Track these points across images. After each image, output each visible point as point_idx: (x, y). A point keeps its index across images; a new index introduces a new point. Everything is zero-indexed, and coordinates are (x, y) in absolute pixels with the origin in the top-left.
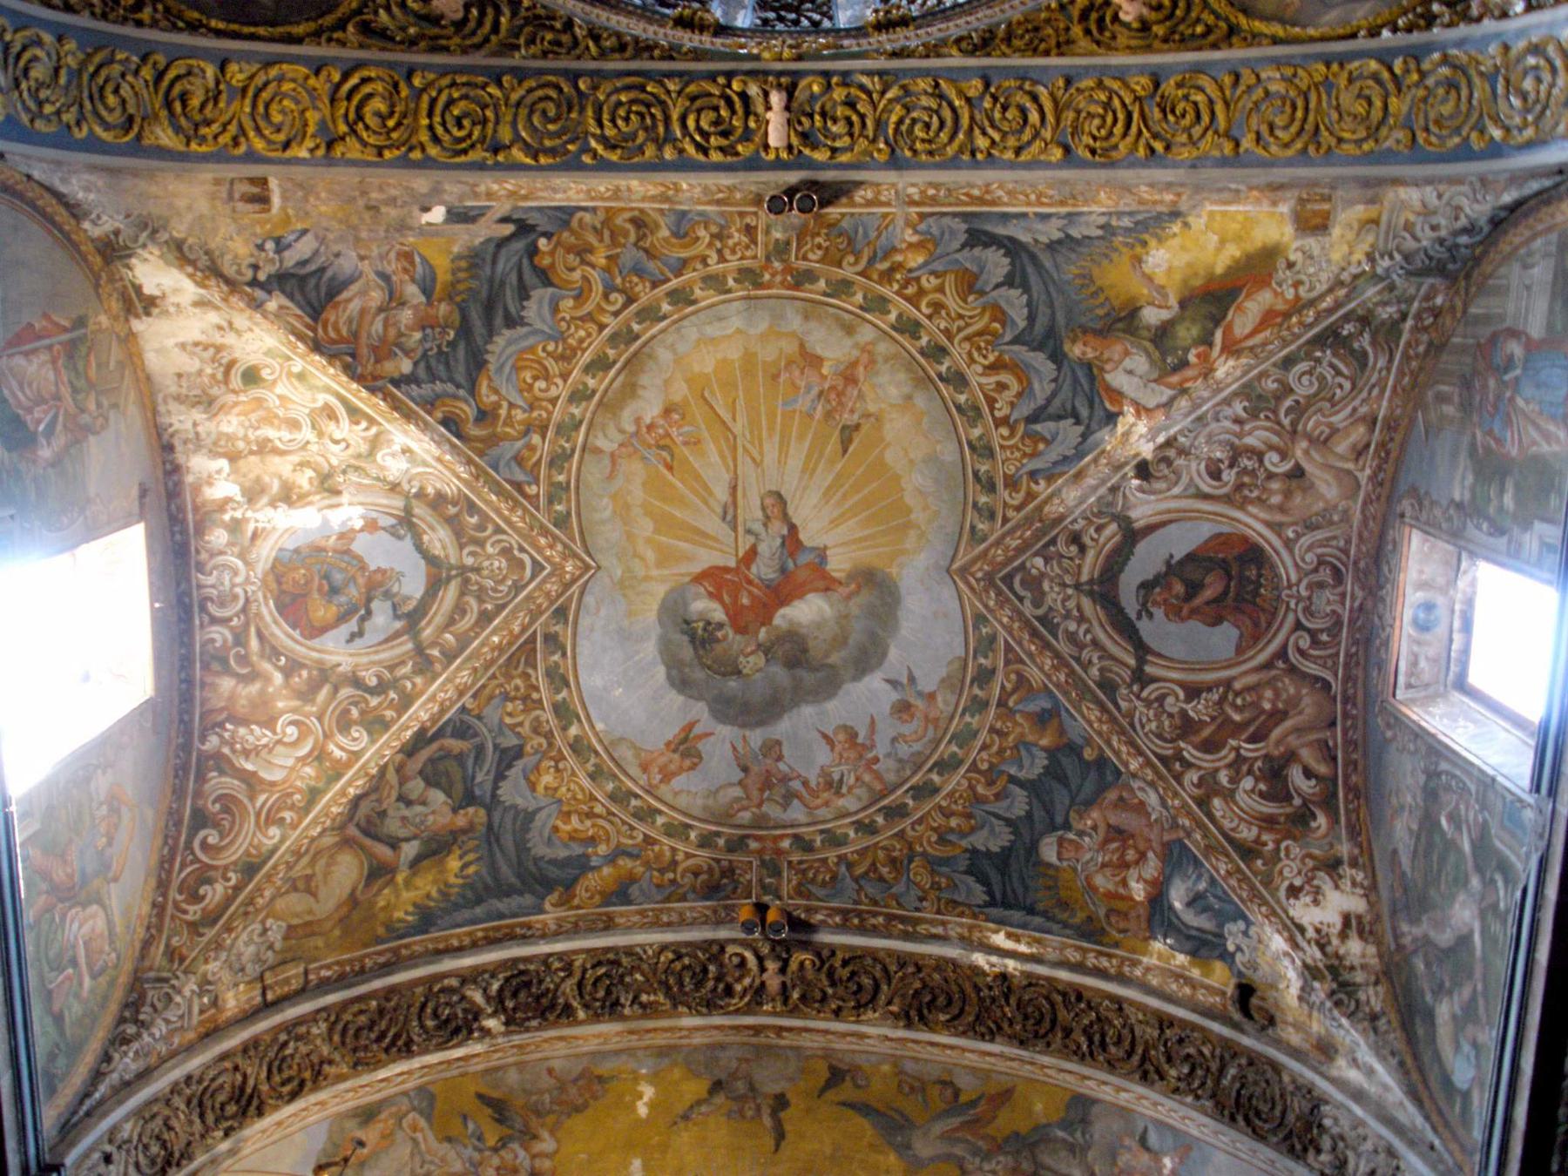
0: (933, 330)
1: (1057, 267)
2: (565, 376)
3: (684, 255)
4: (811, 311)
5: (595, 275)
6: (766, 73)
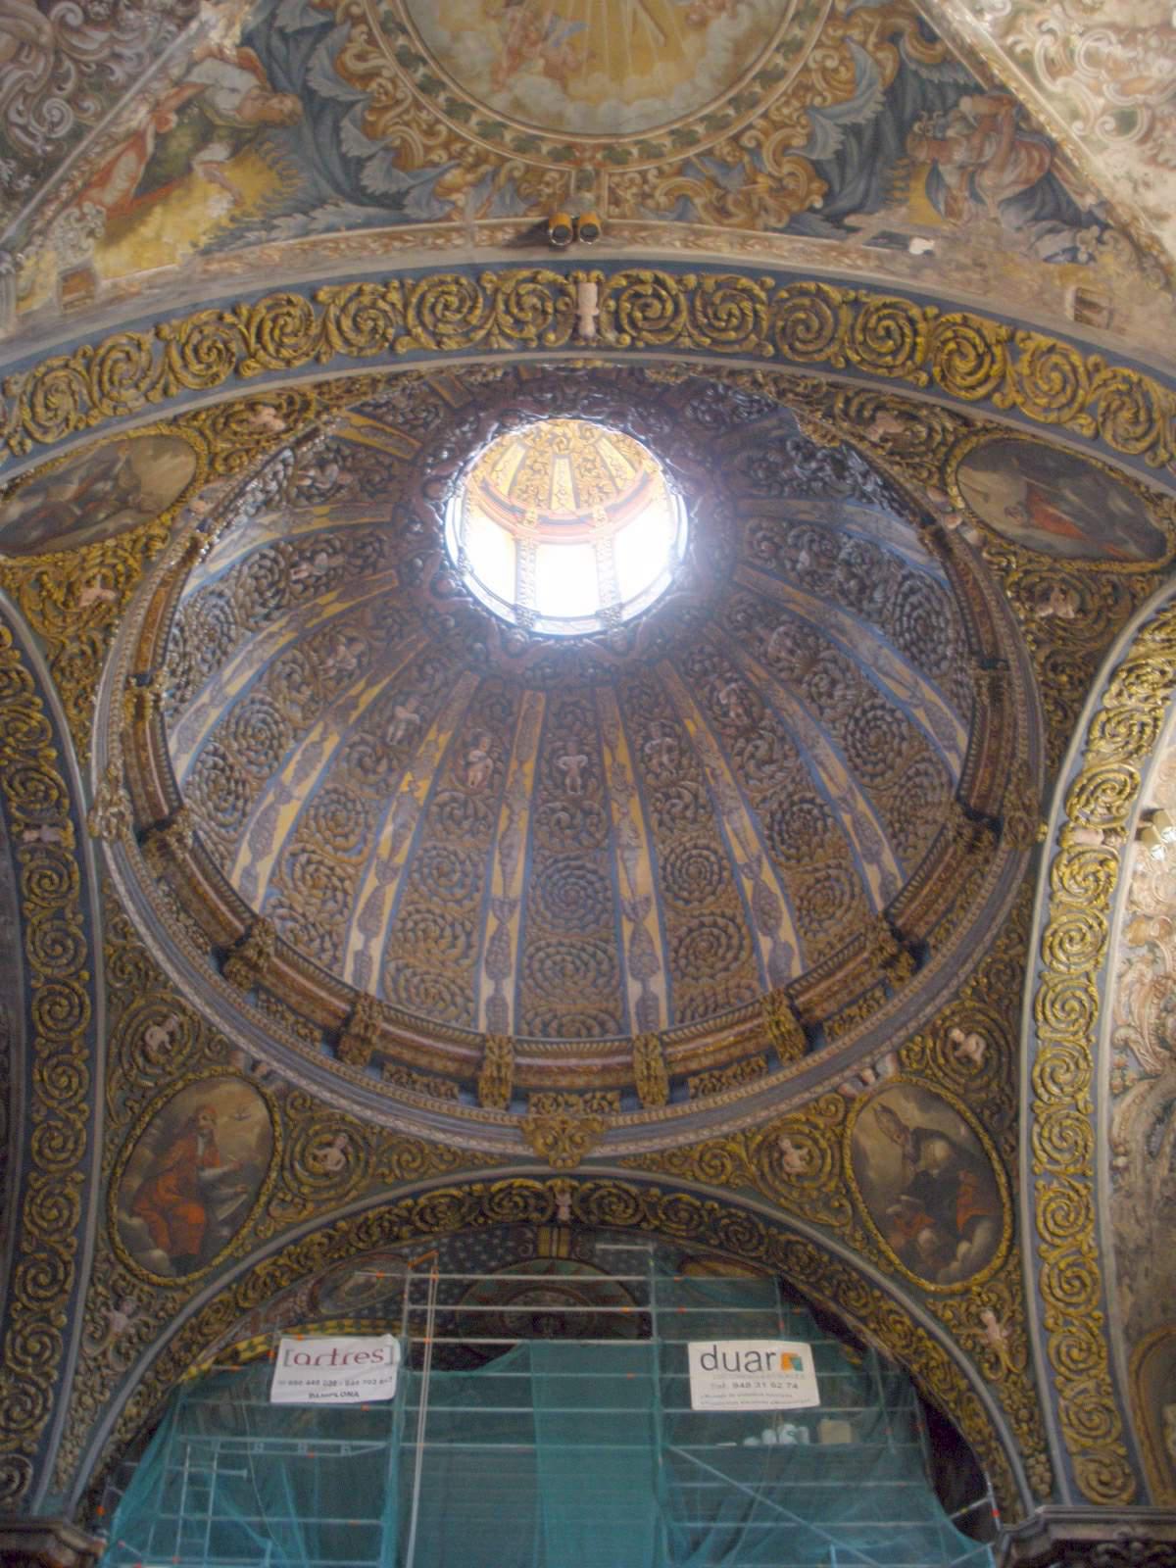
0: (434, 109)
1: (315, 184)
2: (806, 69)
3: (680, 180)
4: (555, 122)
5: (769, 167)
6: (599, 348)
